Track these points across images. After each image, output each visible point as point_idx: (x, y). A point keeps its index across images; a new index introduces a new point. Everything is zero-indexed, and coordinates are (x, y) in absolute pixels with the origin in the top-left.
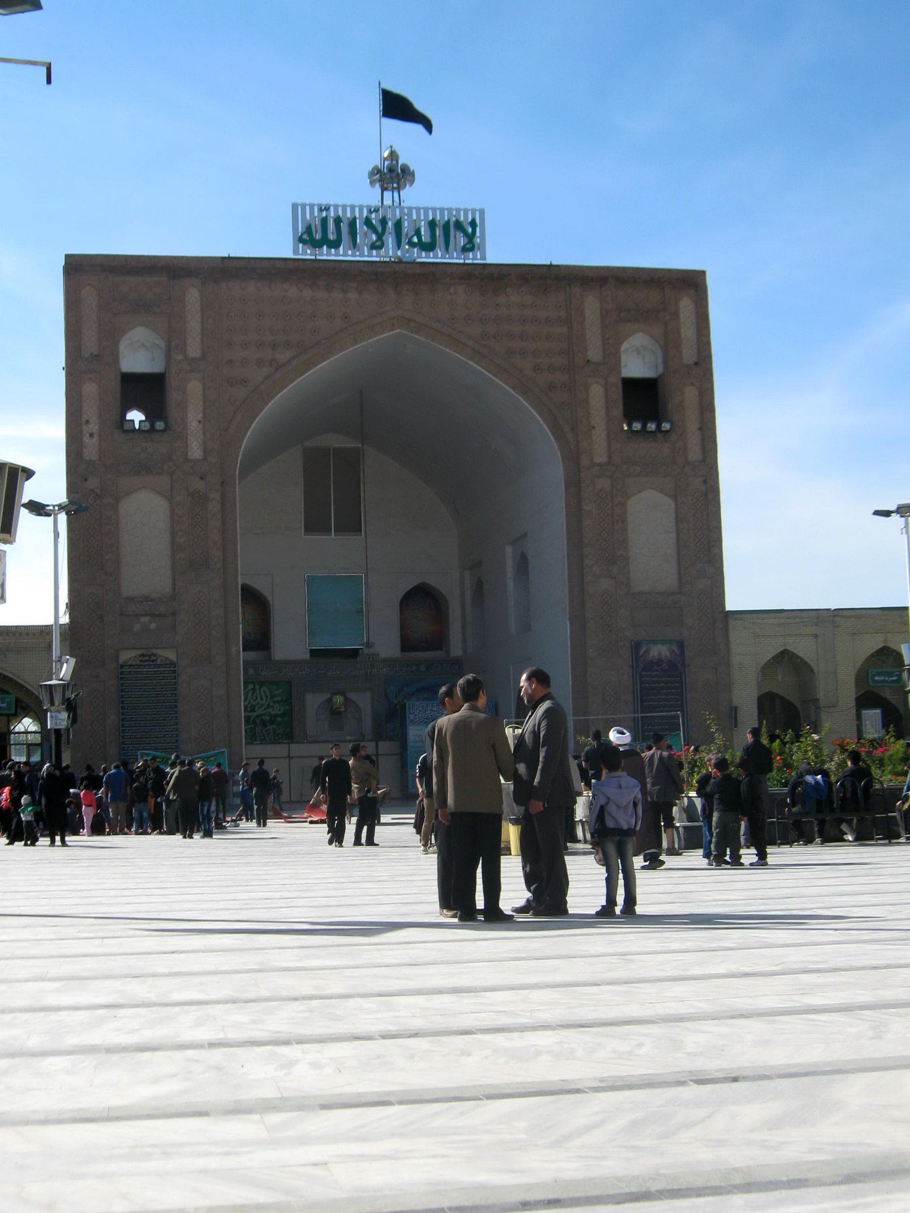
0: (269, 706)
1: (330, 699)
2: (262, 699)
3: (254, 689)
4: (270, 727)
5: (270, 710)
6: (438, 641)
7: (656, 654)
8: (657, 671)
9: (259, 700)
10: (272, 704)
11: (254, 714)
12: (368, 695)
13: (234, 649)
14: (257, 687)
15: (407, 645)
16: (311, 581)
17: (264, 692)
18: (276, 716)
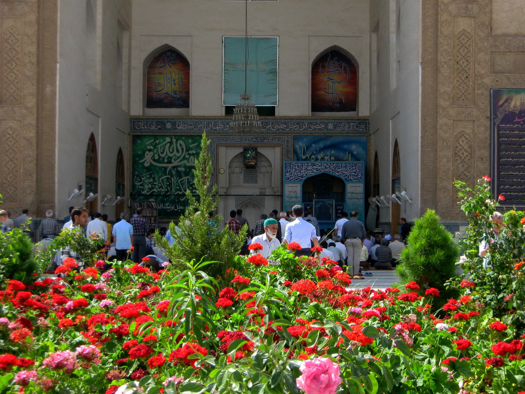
0: (184, 158)
2: (178, 151)
3: (171, 143)
4: (185, 178)
6: (350, 103)
7: (518, 104)
8: (518, 123)
10: (187, 156)
11: (170, 166)
12: (278, 150)
13: (48, 89)
14: (174, 140)
15: (318, 104)
16: (227, 42)
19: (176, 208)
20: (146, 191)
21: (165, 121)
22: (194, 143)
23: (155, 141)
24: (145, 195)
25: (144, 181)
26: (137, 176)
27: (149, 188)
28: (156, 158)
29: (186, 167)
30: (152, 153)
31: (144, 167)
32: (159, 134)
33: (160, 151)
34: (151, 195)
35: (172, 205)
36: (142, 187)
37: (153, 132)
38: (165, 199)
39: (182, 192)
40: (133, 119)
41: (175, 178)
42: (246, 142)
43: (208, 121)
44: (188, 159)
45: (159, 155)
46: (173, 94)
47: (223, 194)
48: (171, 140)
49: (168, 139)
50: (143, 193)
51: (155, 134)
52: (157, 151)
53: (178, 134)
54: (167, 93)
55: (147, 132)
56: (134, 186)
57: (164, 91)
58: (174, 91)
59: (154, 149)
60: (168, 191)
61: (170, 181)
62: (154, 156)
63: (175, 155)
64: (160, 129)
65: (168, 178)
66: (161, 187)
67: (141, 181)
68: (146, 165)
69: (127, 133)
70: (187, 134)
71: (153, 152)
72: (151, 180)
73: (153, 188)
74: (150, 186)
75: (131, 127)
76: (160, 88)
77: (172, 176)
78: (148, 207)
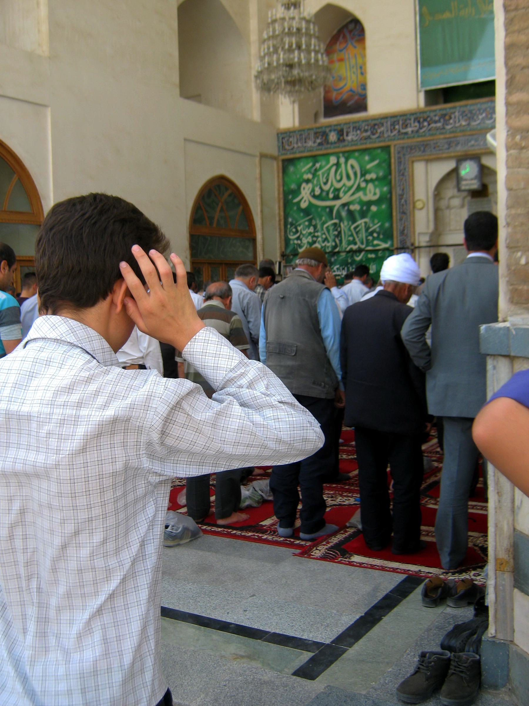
0: (359, 189)
1: (455, 171)
3: (338, 165)
4: (361, 222)
5: (360, 194)
10: (363, 185)
11: (337, 203)
14: (342, 160)
17: (352, 167)
18: (369, 203)
22: (372, 160)
23: (314, 165)
25: (301, 233)
26: (292, 224)
27: (308, 242)
29: (361, 203)
30: (310, 185)
31: (300, 210)
33: (322, 180)
35: (343, 269)
36: (299, 242)
38: (333, 260)
41: (346, 223)
42: (459, 148)
44: (364, 189)
47: (423, 244)
49: (333, 160)
52: (318, 180)
53: (348, 149)
54: (351, 90)
55: (302, 152)
56: (287, 241)
57: (347, 88)
59: (313, 178)
60: (336, 246)
61: (339, 229)
62: (313, 191)
64: (320, 144)
65: (335, 224)
66: (326, 240)
67: (297, 231)
68: (304, 205)
69: (258, 154)
72: (311, 230)
73: (314, 242)
74: (310, 239)
76: (341, 84)
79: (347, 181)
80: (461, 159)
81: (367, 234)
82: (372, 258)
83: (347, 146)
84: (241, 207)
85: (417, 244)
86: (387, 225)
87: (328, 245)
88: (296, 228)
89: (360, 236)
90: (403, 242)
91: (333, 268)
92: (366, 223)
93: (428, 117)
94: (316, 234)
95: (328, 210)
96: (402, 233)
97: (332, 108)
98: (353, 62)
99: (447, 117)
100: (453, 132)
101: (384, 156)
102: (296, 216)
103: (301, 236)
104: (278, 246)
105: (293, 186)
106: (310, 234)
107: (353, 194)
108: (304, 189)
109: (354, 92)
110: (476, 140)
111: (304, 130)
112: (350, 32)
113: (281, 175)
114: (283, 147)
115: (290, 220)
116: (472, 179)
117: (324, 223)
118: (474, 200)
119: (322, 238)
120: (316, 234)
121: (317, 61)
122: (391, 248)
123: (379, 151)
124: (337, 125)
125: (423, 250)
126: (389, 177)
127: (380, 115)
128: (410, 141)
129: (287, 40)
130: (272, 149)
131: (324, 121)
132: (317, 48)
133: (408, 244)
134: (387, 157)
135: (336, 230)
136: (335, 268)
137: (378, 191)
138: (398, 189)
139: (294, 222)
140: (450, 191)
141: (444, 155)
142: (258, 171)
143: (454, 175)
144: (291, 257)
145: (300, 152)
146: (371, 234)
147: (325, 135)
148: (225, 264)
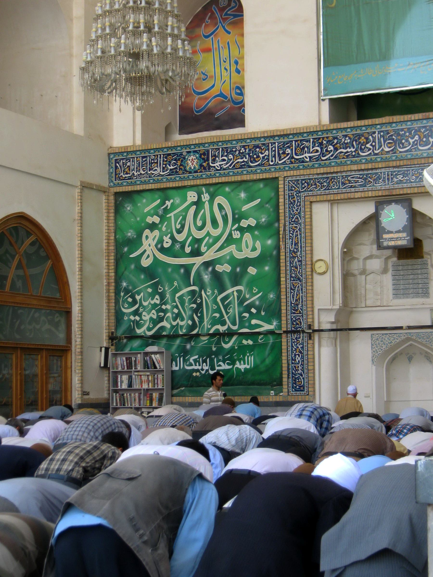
0: (230, 240)
1: (375, 218)
2: (214, 223)
3: (198, 203)
5: (232, 248)
9: (209, 227)
10: (236, 235)
14: (206, 197)
17: (221, 207)
18: (246, 263)
19: (213, 368)
20: (145, 328)
21: (184, 151)
22: (251, 199)
24: (141, 337)
25: (141, 304)
27: (151, 319)
28: (166, 245)
29: (233, 261)
30: (156, 233)
32: (171, 185)
33: (175, 225)
34: (156, 338)
35: (205, 361)
36: (137, 318)
37: (158, 182)
38: (188, 346)
39: (226, 327)
40: (115, 154)
41: (209, 292)
43: (282, 140)
44: (238, 242)
45: (173, 238)
46: (234, 96)
48: (199, 198)
49: (192, 196)
50: (139, 331)
51: (163, 186)
52: (169, 226)
53: (214, 181)
54: (221, 95)
55: (145, 183)
56: (119, 316)
57: (215, 91)
58: (238, 88)
59: (161, 222)
60: (194, 326)
62: (161, 241)
63: (208, 234)
64: (173, 172)
65: (193, 292)
66: (178, 316)
67: (135, 302)
68: (146, 263)
70: (233, 179)
71: (160, 230)
72: (157, 300)
73: (161, 319)
75: (110, 174)
76: (206, 85)
77: (202, 286)
78: (146, 365)
79: (212, 227)
80: (382, 202)
81: (241, 309)
82: (248, 345)
83: (214, 176)
84: (49, 263)
85: (316, 328)
86: (272, 296)
87: (181, 323)
88: (133, 297)
89: (231, 310)
90: (295, 322)
91: (189, 359)
92: (239, 291)
93: (335, 138)
94: (164, 307)
95: (182, 271)
96: (295, 309)
97: (191, 120)
98: (225, 53)
99: (363, 140)
100: (371, 161)
101: (269, 193)
102: (134, 279)
103: (141, 310)
104: (105, 323)
105: (130, 234)
106: (155, 305)
107: (221, 248)
108: (147, 237)
109: (226, 97)
110: (405, 175)
111: (148, 150)
112: (222, 10)
113: (112, 215)
114: (116, 175)
115: (124, 284)
116: (399, 232)
117: (176, 290)
118: (402, 261)
119: (173, 313)
120: (164, 307)
121: (175, 49)
122: (277, 332)
123: (261, 185)
124: (199, 145)
125: (325, 335)
126: (276, 225)
127: (264, 132)
128: (308, 172)
129: (131, 18)
130: (100, 176)
131: (179, 138)
132: (176, 32)
133: (304, 326)
134: (273, 194)
135: (195, 302)
136: (191, 360)
137: (258, 244)
138: (289, 241)
139: (130, 288)
140: (366, 247)
141: (358, 195)
142: (77, 209)
143: (373, 224)
144: (125, 341)
145: (142, 183)
146: (248, 309)
147: (180, 158)
148: (22, 348)
